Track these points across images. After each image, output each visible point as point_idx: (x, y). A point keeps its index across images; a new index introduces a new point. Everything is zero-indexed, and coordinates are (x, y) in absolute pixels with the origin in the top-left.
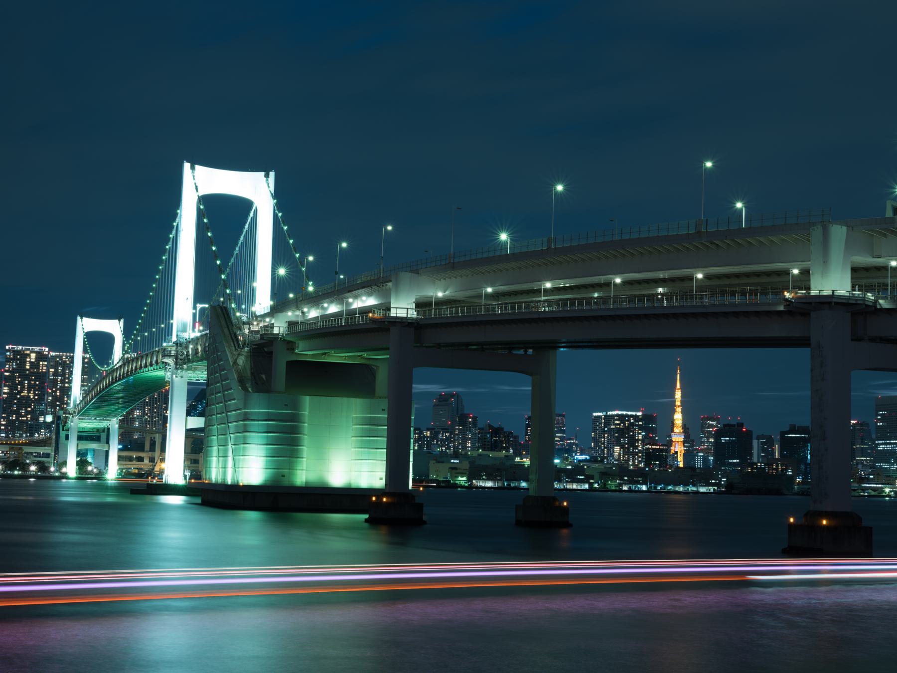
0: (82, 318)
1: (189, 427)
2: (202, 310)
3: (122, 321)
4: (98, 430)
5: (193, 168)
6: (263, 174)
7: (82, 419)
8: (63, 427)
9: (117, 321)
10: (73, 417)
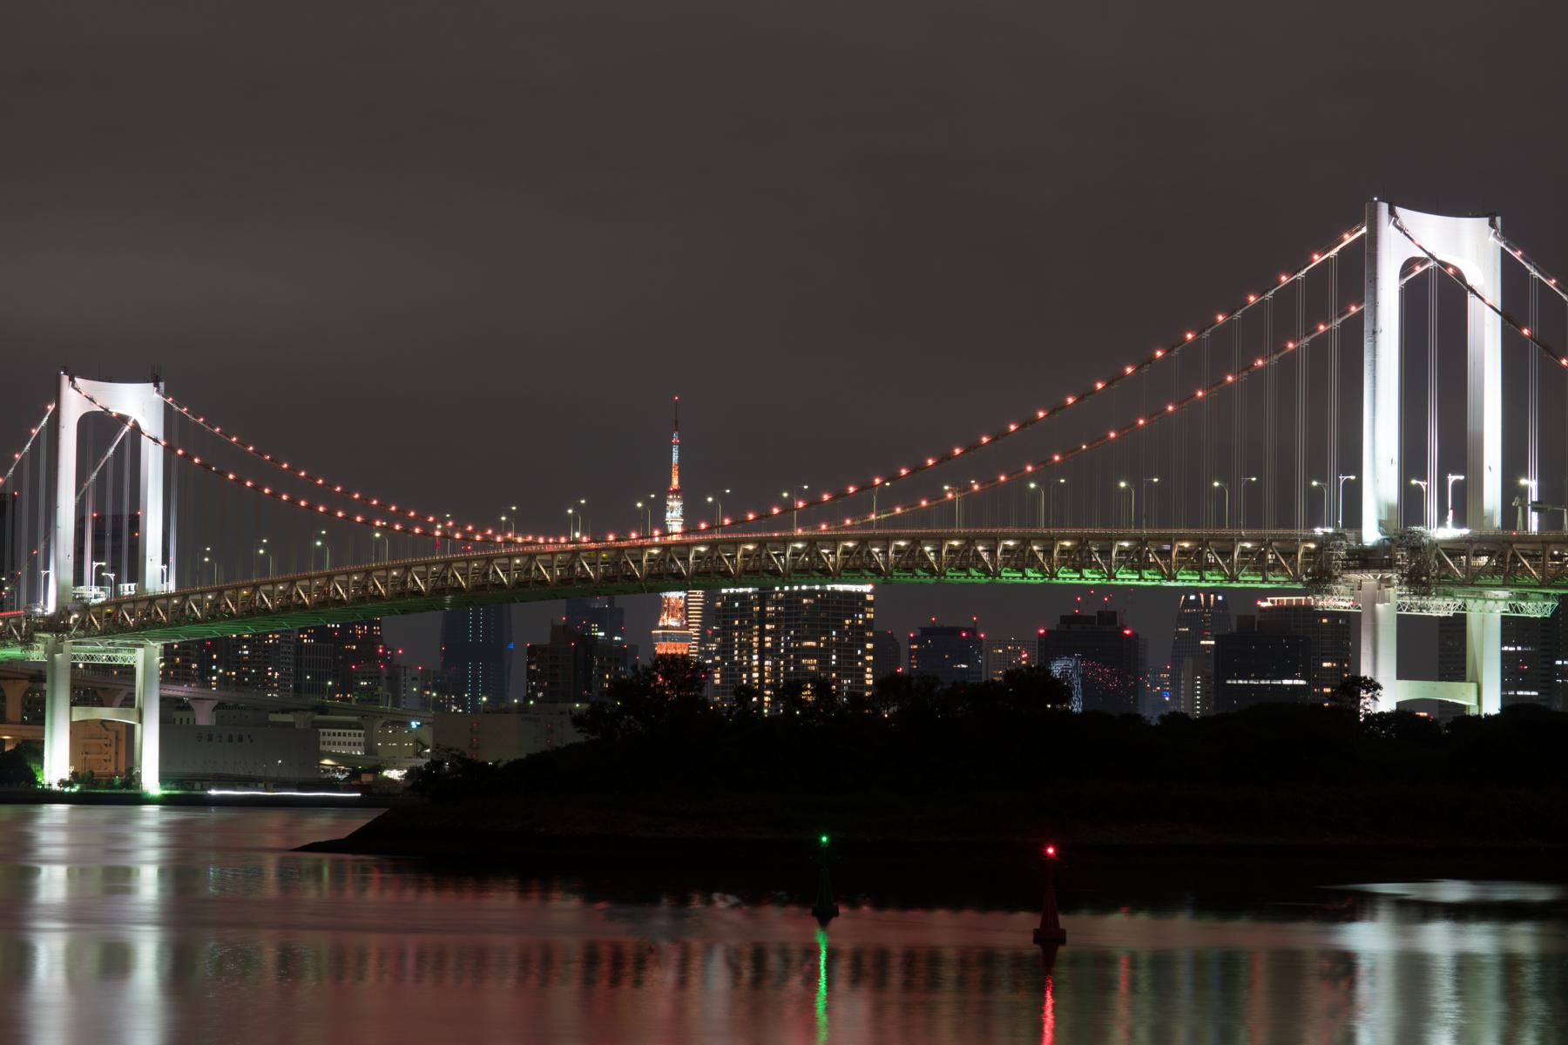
0: (74, 382)
1: (1398, 701)
2: (1456, 483)
3: (162, 385)
5: (1392, 213)
6: (1486, 220)
7: (80, 644)
9: (152, 384)
10: (63, 640)
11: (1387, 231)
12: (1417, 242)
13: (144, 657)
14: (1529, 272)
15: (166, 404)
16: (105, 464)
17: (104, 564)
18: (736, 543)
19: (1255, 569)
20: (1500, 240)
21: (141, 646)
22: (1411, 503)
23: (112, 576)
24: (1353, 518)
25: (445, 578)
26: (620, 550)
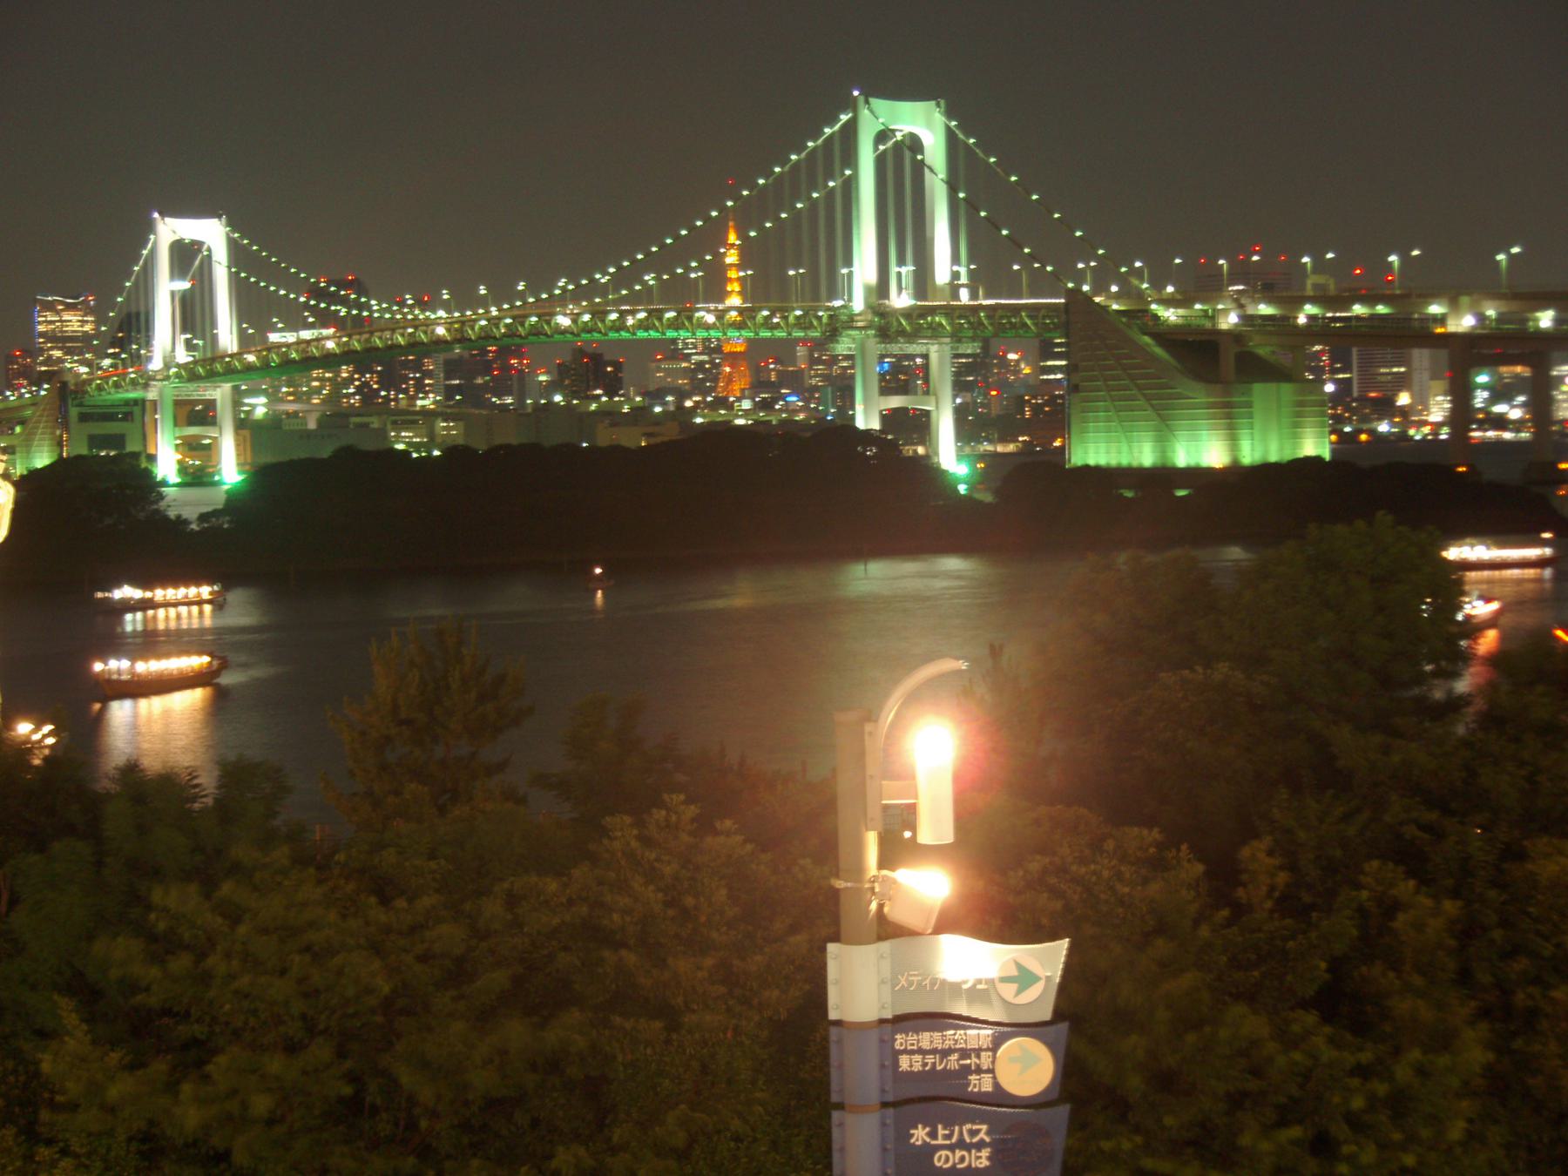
0: (163, 219)
4: (127, 403)
5: (867, 102)
8: (73, 399)
9: (215, 221)
11: (865, 113)
12: (881, 120)
13: (220, 393)
14: (957, 135)
15: (228, 235)
16: (194, 272)
17: (189, 336)
18: (527, 316)
19: (801, 328)
20: (941, 114)
21: (219, 387)
22: (882, 289)
23: (200, 343)
24: (850, 300)
25: (371, 342)
26: (463, 323)
